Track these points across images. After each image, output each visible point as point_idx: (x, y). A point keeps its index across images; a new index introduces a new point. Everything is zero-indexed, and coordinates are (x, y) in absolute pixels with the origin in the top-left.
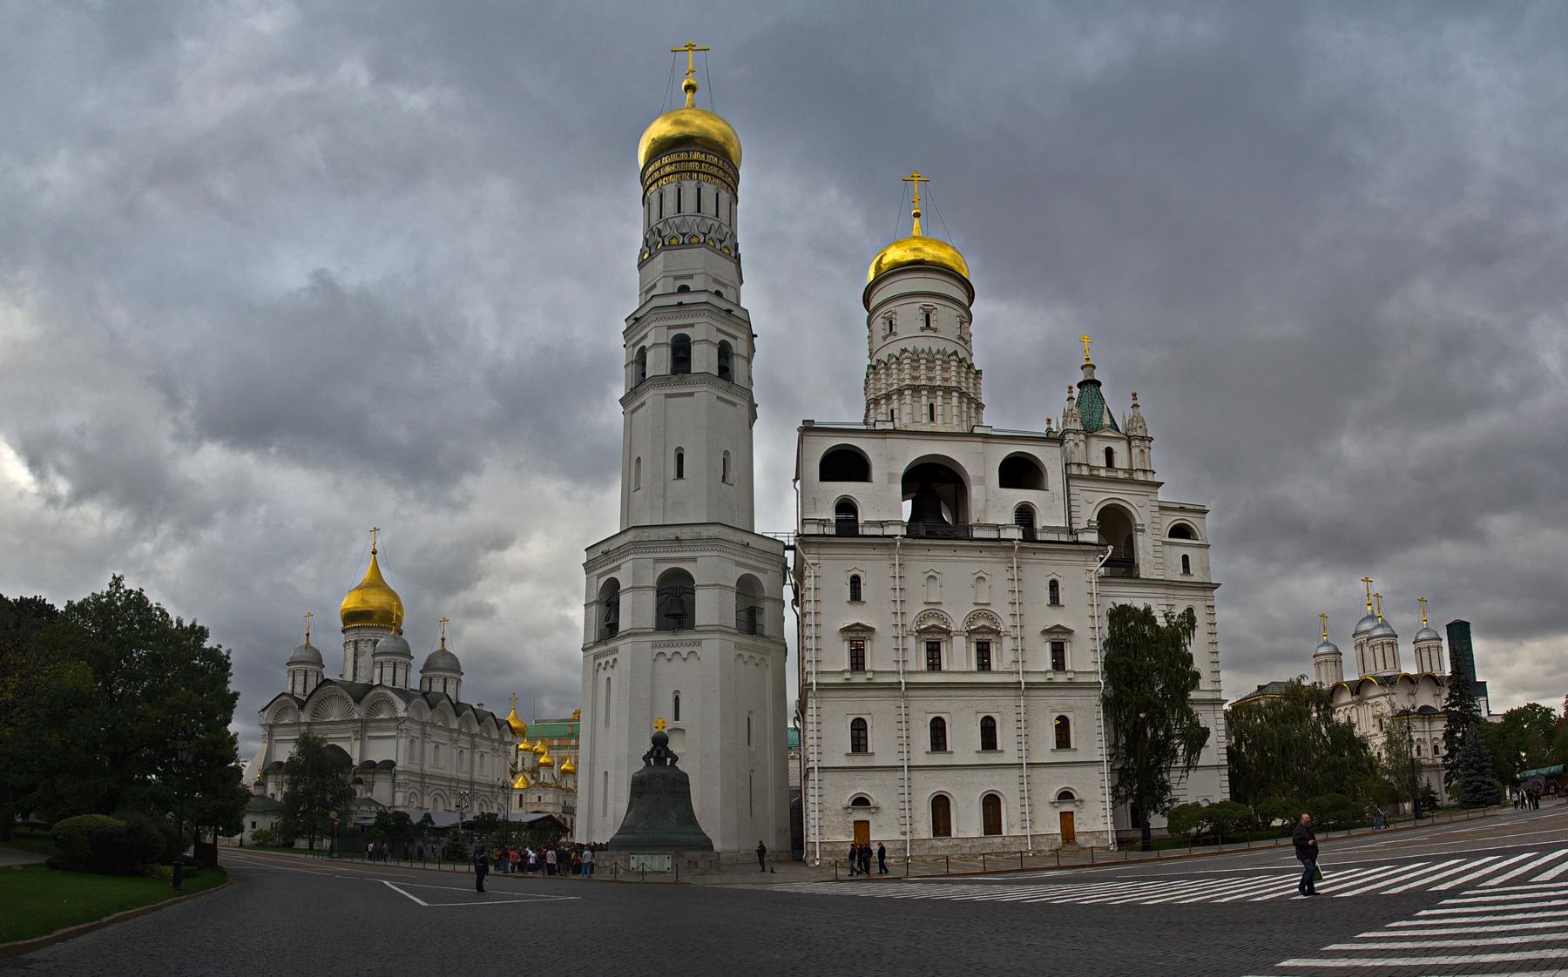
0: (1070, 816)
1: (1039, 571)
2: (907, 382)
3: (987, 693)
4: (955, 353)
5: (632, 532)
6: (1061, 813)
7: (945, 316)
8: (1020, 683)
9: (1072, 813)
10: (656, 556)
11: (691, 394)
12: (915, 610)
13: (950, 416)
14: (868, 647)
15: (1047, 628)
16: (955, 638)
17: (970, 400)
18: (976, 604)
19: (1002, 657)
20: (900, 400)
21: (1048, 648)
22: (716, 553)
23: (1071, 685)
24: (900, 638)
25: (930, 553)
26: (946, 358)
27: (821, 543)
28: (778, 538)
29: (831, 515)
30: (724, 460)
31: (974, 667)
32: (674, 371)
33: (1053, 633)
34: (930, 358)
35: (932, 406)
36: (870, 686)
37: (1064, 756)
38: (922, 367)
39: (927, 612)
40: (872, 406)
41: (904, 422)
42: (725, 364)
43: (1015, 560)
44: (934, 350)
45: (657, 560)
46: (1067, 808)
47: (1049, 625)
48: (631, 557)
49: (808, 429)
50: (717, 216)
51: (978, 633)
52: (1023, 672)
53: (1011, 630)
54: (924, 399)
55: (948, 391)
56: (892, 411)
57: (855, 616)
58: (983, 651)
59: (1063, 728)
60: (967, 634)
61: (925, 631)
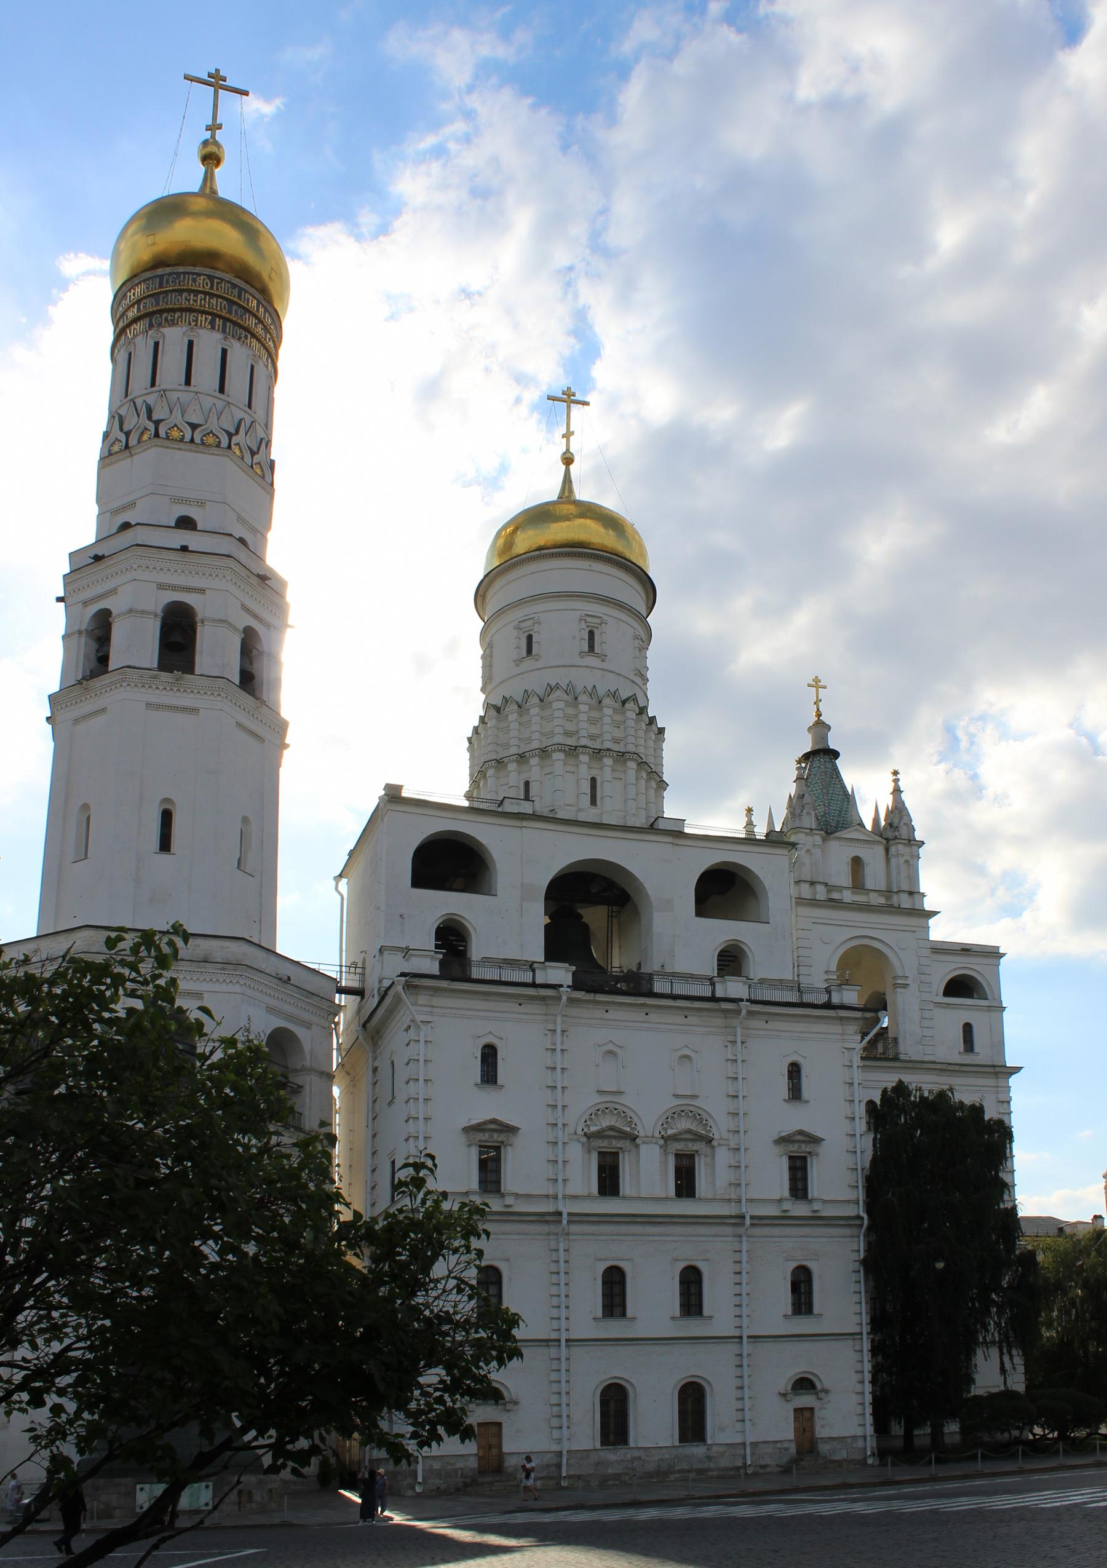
3: (689, 1230)
11: (194, 710)
16: (643, 1148)
18: (676, 1096)
25: (607, 1016)
28: (321, 971)
39: (602, 1106)
49: (393, 795)
50: (250, 406)
60: (662, 1142)
61: (599, 1135)
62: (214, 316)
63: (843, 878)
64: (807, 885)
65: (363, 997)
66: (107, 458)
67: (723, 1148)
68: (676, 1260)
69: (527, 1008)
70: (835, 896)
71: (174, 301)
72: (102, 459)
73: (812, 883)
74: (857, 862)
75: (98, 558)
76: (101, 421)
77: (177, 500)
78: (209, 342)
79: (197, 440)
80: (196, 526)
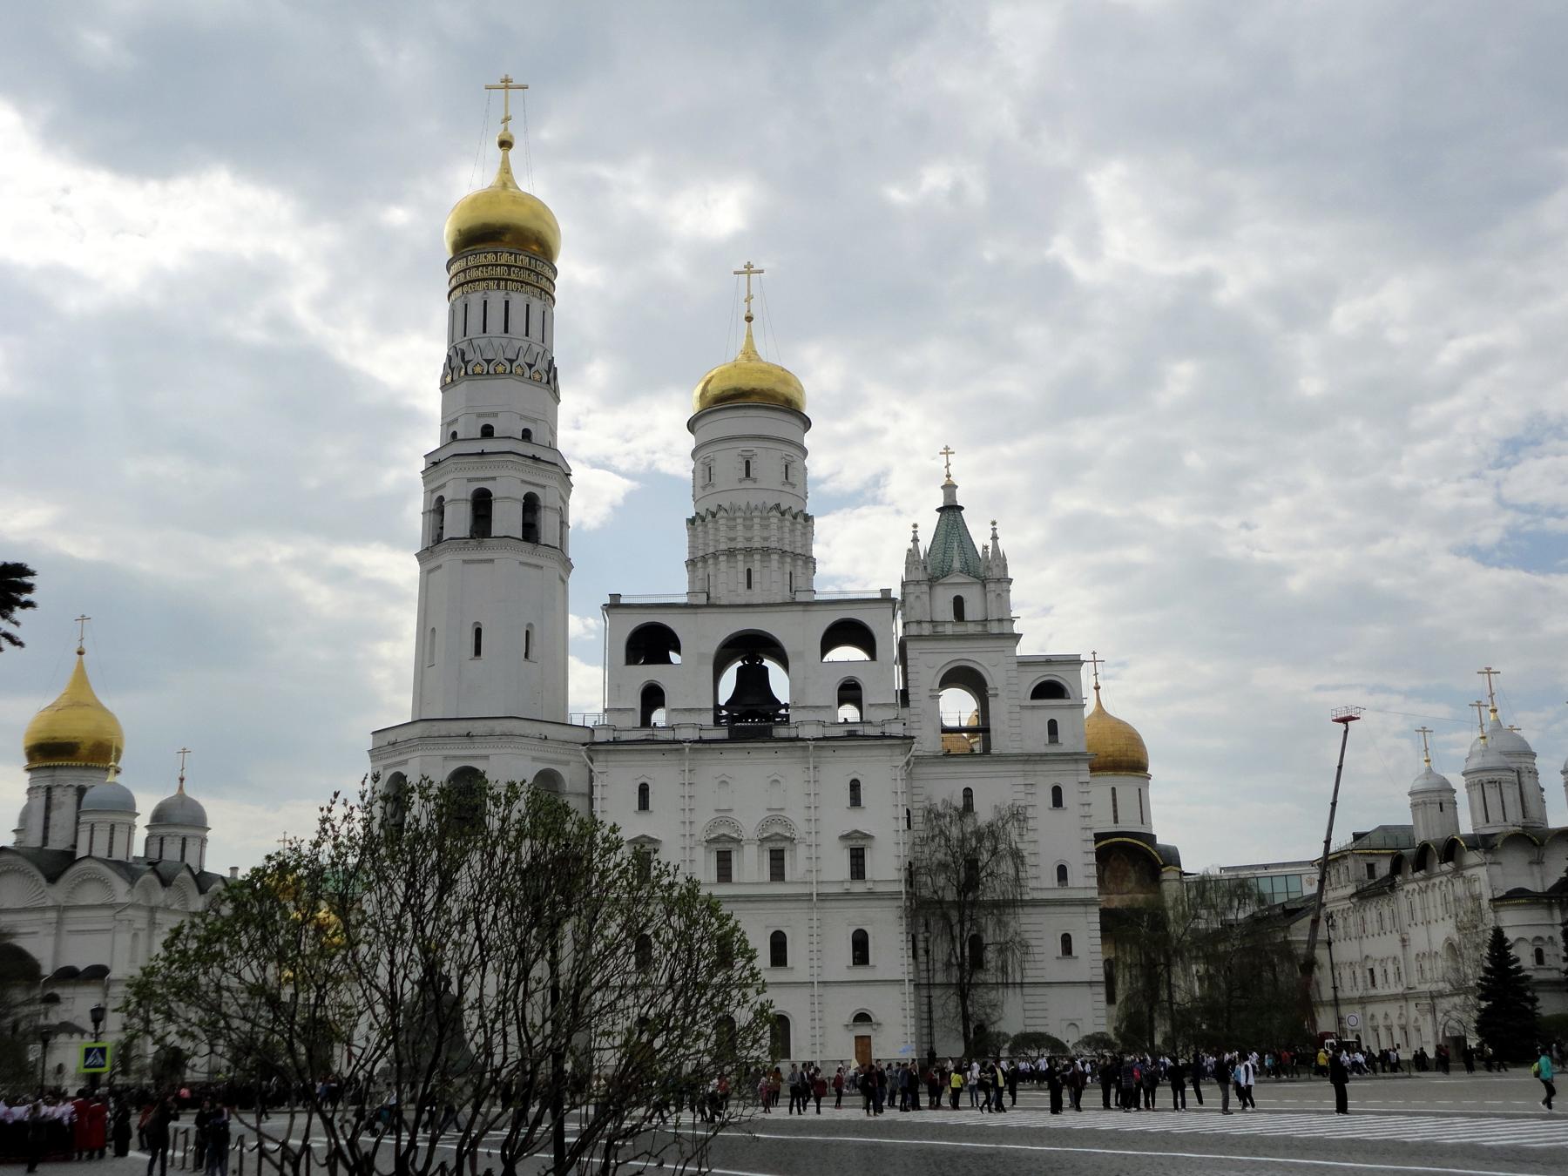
0: (866, 1040)
1: (838, 770)
2: (723, 547)
3: (778, 905)
4: (778, 506)
5: (421, 724)
6: (856, 1037)
7: (768, 462)
8: (812, 894)
9: (869, 1037)
10: (446, 752)
12: (704, 818)
13: (771, 583)
15: (845, 833)
16: (746, 847)
17: (795, 556)
19: (795, 866)
20: (716, 564)
22: (510, 751)
23: (871, 895)
24: (688, 849)
26: (765, 514)
27: (609, 751)
30: (527, 632)
31: (767, 877)
32: (472, 537)
33: (852, 839)
34: (748, 515)
35: (749, 571)
37: (861, 973)
38: (740, 527)
41: (722, 594)
42: (529, 520)
43: (811, 759)
44: (753, 505)
45: (446, 758)
46: (863, 1030)
47: (847, 830)
48: (419, 753)
49: (614, 605)
51: (772, 841)
52: (817, 883)
53: (806, 836)
55: (766, 552)
58: (777, 858)
59: (861, 948)
62: (499, 279)
63: (945, 612)
64: (915, 624)
66: (444, 387)
67: (803, 845)
68: (767, 927)
69: (668, 756)
70: (940, 629)
71: (474, 274)
72: (442, 388)
73: (919, 622)
74: (959, 603)
75: (435, 464)
76: (444, 359)
77: (480, 415)
78: (496, 298)
79: (492, 371)
80: (493, 432)
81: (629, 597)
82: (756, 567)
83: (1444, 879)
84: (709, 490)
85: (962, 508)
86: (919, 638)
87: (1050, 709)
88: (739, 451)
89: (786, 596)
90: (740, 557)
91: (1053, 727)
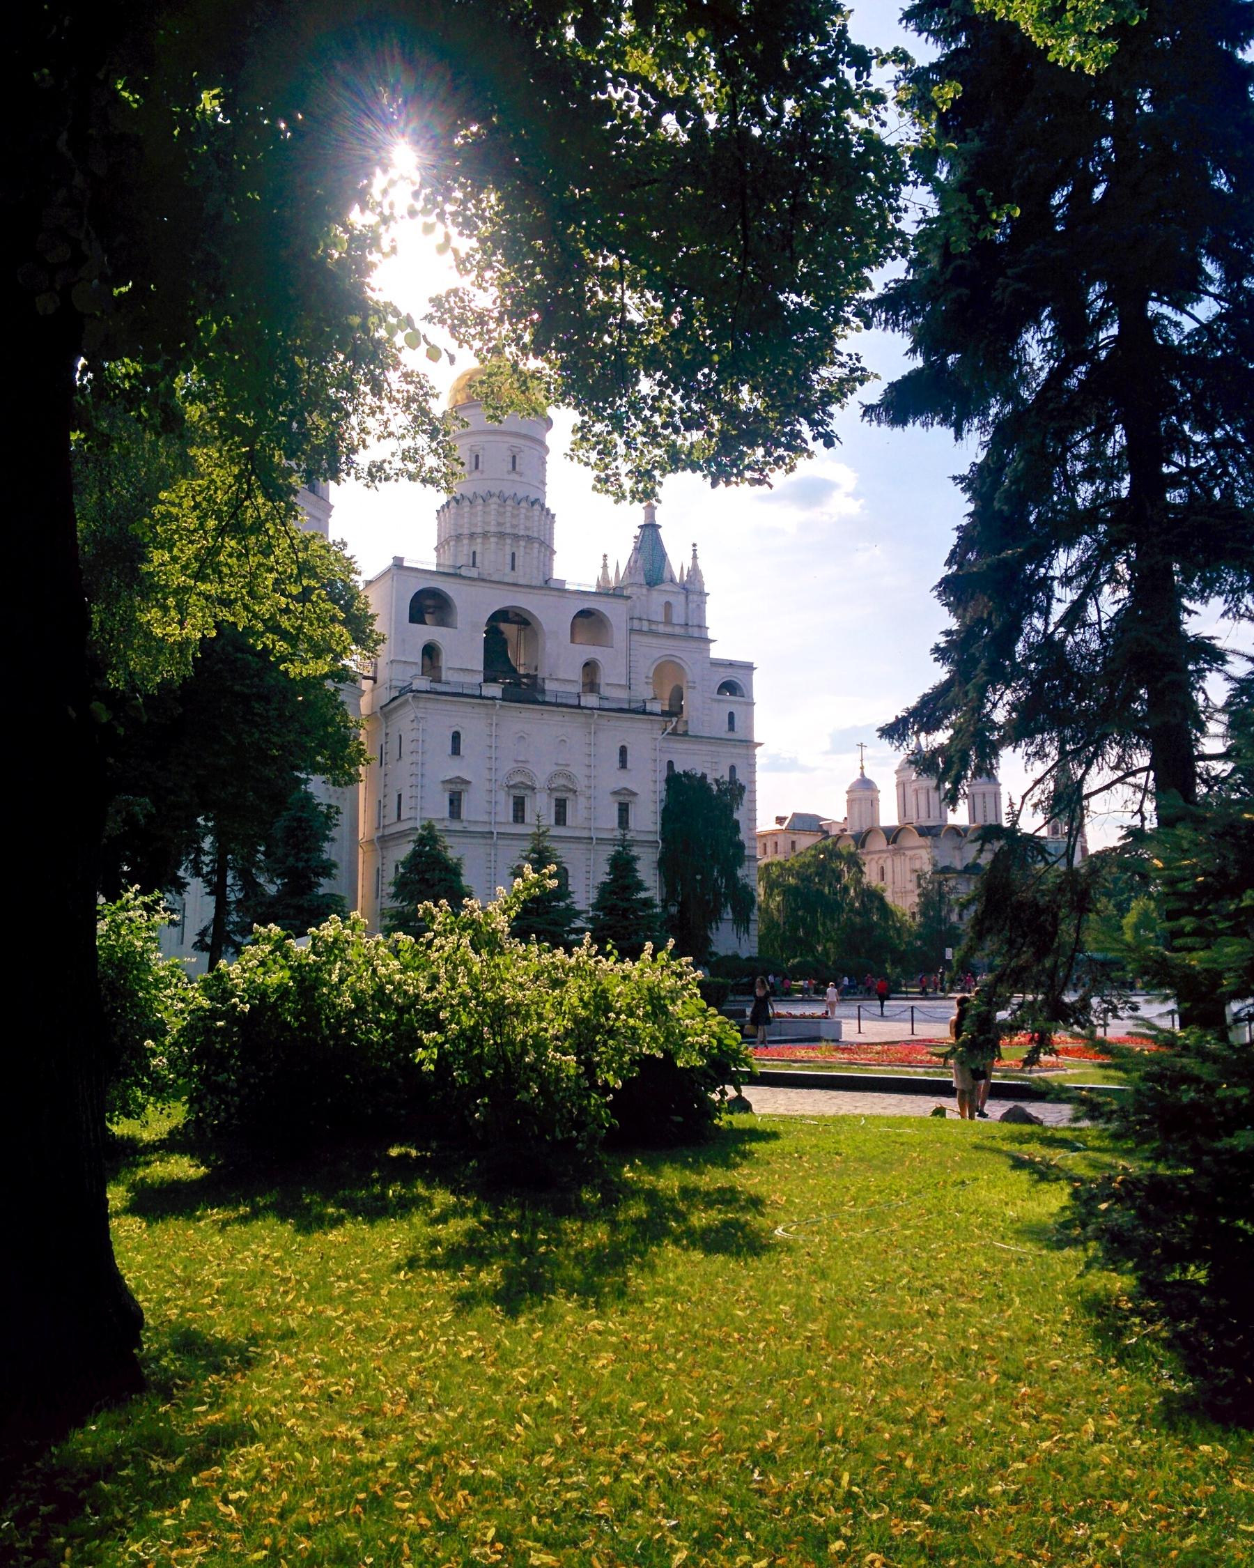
2: (493, 529)
4: (537, 500)
14: (464, 797)
16: (538, 795)
20: (483, 544)
21: (615, 809)
29: (417, 657)
35: (513, 554)
36: (466, 833)
38: (508, 514)
40: (452, 543)
54: (508, 548)
55: (529, 539)
56: (474, 553)
57: (454, 769)
58: (561, 805)
61: (514, 787)
65: (375, 682)
70: (654, 627)
73: (640, 619)
74: (668, 605)
81: (411, 561)
82: (520, 553)
83: (885, 855)
84: (476, 475)
85: (660, 527)
86: (640, 632)
87: (730, 703)
88: (506, 445)
89: (538, 582)
90: (508, 541)
91: (731, 715)
